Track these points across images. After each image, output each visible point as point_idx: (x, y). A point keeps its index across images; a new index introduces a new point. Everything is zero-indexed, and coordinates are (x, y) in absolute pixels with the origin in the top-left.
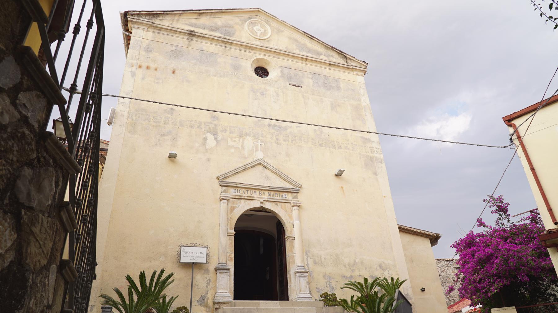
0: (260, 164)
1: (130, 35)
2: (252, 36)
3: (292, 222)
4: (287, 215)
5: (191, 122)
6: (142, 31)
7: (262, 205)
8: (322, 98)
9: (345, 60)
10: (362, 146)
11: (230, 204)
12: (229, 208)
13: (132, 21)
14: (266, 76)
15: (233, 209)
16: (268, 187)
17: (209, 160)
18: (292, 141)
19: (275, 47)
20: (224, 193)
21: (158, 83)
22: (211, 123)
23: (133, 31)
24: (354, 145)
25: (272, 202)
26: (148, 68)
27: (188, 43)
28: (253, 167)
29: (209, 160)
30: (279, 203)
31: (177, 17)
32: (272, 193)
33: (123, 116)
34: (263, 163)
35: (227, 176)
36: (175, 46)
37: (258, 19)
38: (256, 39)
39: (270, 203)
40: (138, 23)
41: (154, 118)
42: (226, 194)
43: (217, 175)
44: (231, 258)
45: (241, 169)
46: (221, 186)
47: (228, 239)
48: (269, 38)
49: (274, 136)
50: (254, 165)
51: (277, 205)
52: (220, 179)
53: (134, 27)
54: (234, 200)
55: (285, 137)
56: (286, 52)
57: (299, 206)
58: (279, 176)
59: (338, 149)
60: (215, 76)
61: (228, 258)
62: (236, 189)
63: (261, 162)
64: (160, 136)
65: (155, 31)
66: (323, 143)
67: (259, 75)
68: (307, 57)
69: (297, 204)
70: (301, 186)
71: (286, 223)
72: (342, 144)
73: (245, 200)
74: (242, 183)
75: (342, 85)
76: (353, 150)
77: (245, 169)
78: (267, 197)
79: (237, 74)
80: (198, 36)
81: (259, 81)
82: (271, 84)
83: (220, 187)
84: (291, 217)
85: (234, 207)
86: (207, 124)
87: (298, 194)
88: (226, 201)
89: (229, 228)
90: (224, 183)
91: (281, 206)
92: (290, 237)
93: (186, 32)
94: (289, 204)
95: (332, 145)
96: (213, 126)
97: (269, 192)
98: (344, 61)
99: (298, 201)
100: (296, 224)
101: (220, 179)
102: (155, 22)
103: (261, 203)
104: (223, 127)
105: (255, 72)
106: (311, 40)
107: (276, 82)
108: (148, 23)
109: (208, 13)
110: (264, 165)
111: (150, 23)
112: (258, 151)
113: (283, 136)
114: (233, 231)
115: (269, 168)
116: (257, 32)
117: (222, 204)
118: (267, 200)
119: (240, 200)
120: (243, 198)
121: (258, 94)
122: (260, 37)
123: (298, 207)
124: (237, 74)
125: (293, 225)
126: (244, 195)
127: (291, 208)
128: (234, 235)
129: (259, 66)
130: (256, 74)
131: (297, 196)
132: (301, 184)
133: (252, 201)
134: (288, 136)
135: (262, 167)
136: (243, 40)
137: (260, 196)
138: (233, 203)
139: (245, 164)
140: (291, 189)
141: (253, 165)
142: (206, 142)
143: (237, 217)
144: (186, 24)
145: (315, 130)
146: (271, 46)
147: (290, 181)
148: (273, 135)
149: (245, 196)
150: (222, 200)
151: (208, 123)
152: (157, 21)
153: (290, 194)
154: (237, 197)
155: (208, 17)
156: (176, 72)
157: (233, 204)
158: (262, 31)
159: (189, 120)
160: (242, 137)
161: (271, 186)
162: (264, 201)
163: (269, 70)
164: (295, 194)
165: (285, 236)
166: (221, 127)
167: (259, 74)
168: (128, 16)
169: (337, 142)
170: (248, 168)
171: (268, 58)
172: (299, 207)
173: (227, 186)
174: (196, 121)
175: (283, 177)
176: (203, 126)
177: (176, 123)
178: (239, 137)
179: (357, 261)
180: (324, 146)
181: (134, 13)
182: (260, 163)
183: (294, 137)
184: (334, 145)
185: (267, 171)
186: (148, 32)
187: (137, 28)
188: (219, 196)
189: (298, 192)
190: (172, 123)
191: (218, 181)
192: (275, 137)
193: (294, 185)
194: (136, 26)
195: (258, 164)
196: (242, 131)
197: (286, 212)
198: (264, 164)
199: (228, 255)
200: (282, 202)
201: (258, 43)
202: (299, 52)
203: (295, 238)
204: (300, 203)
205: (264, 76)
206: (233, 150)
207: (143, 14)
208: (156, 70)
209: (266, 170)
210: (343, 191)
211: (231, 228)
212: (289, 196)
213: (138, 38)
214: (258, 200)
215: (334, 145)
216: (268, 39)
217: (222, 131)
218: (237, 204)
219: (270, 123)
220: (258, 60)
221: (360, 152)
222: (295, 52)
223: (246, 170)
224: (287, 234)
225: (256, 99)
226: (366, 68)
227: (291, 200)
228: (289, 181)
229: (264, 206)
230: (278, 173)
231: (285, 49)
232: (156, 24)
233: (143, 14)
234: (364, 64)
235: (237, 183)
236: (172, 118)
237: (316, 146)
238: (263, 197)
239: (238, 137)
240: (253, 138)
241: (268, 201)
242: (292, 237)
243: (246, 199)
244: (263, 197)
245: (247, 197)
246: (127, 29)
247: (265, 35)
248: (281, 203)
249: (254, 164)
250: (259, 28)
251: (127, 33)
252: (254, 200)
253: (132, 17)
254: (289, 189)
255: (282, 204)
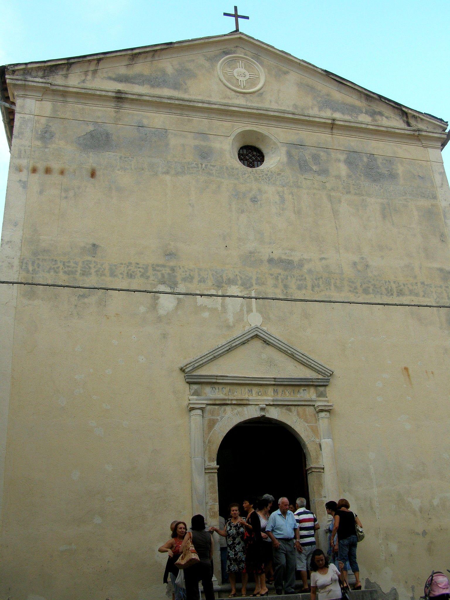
0: (257, 336)
1: (13, 107)
2: (230, 88)
3: (318, 440)
4: (308, 428)
5: (129, 268)
6: (34, 101)
7: (263, 414)
8: (364, 198)
9: (405, 119)
10: (441, 287)
11: (208, 416)
12: (206, 422)
13: (15, 85)
14: (259, 163)
15: (212, 424)
16: (273, 380)
17: (164, 336)
18: (313, 287)
19: (274, 106)
20: (195, 397)
21: (66, 198)
22: (164, 266)
23: (19, 102)
24: (427, 285)
25: (281, 407)
26: (48, 171)
27: (114, 115)
28: (244, 343)
29: (164, 336)
30: (293, 408)
31: (92, 67)
32: (280, 389)
33: (12, 266)
34: (261, 335)
35: (198, 364)
36: (93, 123)
37: (240, 54)
38: (238, 94)
39: (278, 409)
40: (24, 87)
41: (64, 264)
42: (200, 397)
43: (182, 365)
44: (214, 512)
45: (224, 350)
46: (189, 383)
47: (207, 479)
48: (262, 88)
49: (280, 281)
50: (246, 340)
51: (290, 410)
52: (187, 370)
53: (18, 96)
54: (214, 407)
55: (300, 280)
56: (293, 114)
57: (328, 411)
58: (292, 356)
59: (398, 296)
60: (167, 173)
61: (208, 513)
62: (216, 386)
63: (259, 334)
64: (76, 298)
65: (56, 98)
66: (369, 287)
67: (246, 162)
68: (334, 120)
69: (327, 408)
70: (331, 373)
71: (307, 443)
72: (404, 285)
73: (233, 406)
74: (227, 376)
75: (400, 170)
76: (424, 296)
77: (230, 349)
78: (271, 399)
79: (206, 166)
80: (132, 100)
81: (247, 175)
82: (269, 180)
83: (188, 385)
84: (315, 431)
85: (213, 420)
86: (157, 268)
87: (328, 389)
88: (199, 412)
89: (207, 459)
90: (193, 377)
91: (298, 412)
92: (315, 468)
93: (110, 94)
94: (312, 408)
95: (386, 289)
96: (168, 271)
97: (276, 388)
98: (404, 121)
99: (328, 401)
100: (326, 442)
101: (187, 370)
102: (54, 82)
103: (262, 409)
104: (186, 271)
105: (239, 157)
106: (340, 85)
107: (279, 174)
108: (43, 85)
109: (147, 52)
110: (264, 338)
111: (47, 85)
112: (252, 311)
113: (297, 280)
114: (214, 464)
115: (273, 344)
116: (240, 79)
117: (193, 417)
118: (272, 403)
119: (223, 407)
120: (229, 402)
121: (248, 201)
122: (244, 88)
123: (328, 414)
124: (207, 165)
125: (320, 446)
126: (230, 398)
127: (315, 416)
128: (216, 471)
129: (246, 144)
130: (241, 159)
131: (325, 391)
132: (332, 369)
133: (245, 408)
134: (305, 279)
135: (261, 341)
136: (213, 100)
137: (259, 398)
138: (212, 413)
139: (229, 340)
140: (314, 380)
141: (243, 340)
142: (157, 304)
143: (221, 439)
144: (110, 78)
145: (356, 262)
146: (267, 105)
147: (312, 365)
148: (277, 278)
149: (232, 400)
150: (192, 409)
151: (158, 266)
152: (58, 80)
153: (312, 390)
154: (218, 402)
155: (149, 59)
156: (98, 173)
157: (212, 416)
158: (248, 77)
159: (125, 264)
160: (222, 287)
161: (279, 376)
162: (267, 405)
163: (265, 151)
164: (321, 389)
165: (306, 466)
166: (184, 272)
167: (247, 160)
168: (7, 76)
169: (394, 282)
170: (236, 345)
171: (261, 128)
172: (329, 412)
173: (201, 382)
174: (138, 264)
175: (299, 359)
176: (150, 272)
177: (102, 271)
178: (216, 288)
179: (436, 502)
180: (371, 291)
181: (17, 68)
182: (257, 335)
183: (316, 280)
184: (390, 288)
185: (269, 350)
186: (43, 102)
187: (24, 96)
188: (187, 402)
189: (327, 384)
190: (97, 271)
191: (182, 375)
192: (282, 282)
193: (318, 372)
194: (21, 93)
195: (252, 338)
196: (221, 277)
197: (307, 422)
198: (264, 337)
199: (208, 507)
200: (299, 405)
201: (241, 101)
202: (319, 111)
203: (323, 469)
204: (330, 406)
205: (256, 163)
206: (206, 314)
207: (32, 69)
208: (62, 172)
209: (267, 346)
210: (409, 376)
211: (210, 460)
212: (310, 394)
213: (27, 116)
214: (256, 405)
215: (390, 288)
216: (259, 92)
217: (184, 280)
218: (218, 415)
219: (271, 257)
220: (244, 134)
221: (438, 300)
222: (311, 112)
223: (231, 351)
224: (311, 464)
225: (243, 212)
226: (443, 132)
227: (315, 401)
228: (310, 366)
229: (268, 415)
230: (289, 352)
231: (291, 109)
232: (57, 85)
233: (32, 68)
234: (441, 125)
235: (217, 376)
236: (95, 262)
237: (357, 293)
238: (265, 398)
239: (244, 594)
240: (242, 288)
241: (273, 405)
242: (318, 468)
243: (234, 404)
244: (265, 398)
245: (237, 400)
246: (6, 96)
247: (254, 85)
248: (296, 407)
249: (245, 339)
250: (243, 70)
251: (7, 105)
252: (249, 404)
253: (15, 77)
254: (311, 380)
255: (300, 408)
